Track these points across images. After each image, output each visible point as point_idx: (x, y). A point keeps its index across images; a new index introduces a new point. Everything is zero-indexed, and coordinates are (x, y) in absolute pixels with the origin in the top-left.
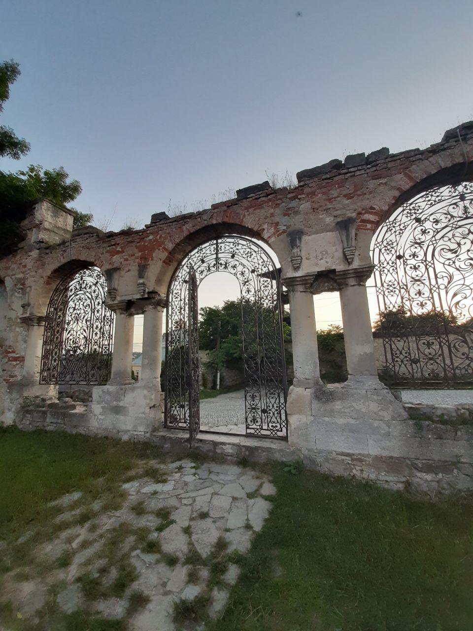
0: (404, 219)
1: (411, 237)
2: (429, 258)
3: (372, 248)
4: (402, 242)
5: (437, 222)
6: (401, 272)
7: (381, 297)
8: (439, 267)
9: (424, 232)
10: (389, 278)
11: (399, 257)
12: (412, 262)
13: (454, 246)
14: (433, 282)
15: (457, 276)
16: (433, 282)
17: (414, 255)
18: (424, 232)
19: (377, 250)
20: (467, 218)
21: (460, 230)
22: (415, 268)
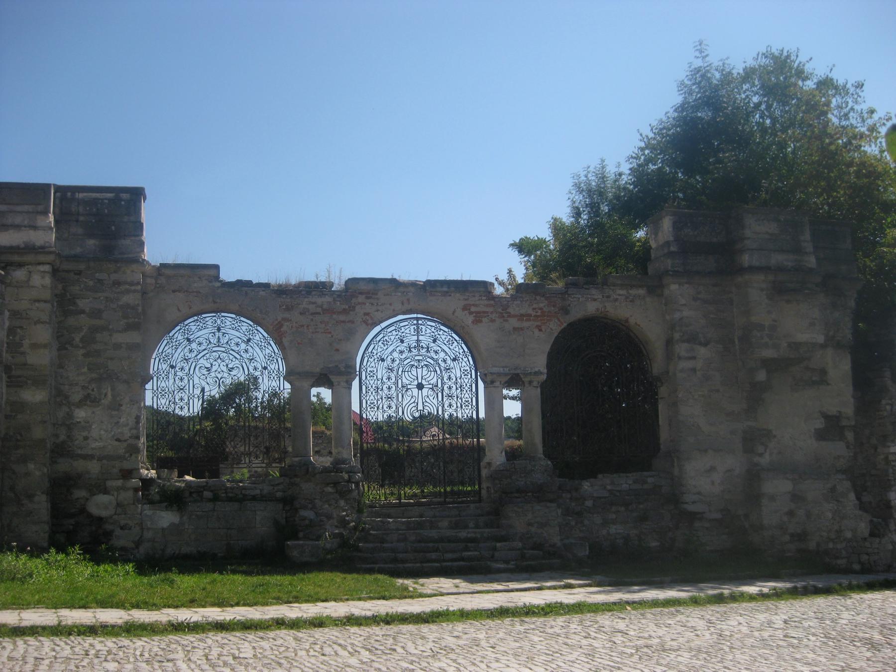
0: (180, 337)
1: (182, 354)
2: (191, 372)
3: (154, 357)
4: (176, 355)
5: (200, 344)
6: (171, 381)
7: (155, 398)
8: (196, 380)
9: (191, 351)
10: (163, 384)
11: (172, 367)
12: (180, 374)
13: (209, 366)
14: (191, 392)
15: (207, 389)
16: (191, 392)
17: (182, 369)
18: (191, 351)
19: (157, 359)
20: (219, 346)
21: (214, 354)
22: (181, 379)
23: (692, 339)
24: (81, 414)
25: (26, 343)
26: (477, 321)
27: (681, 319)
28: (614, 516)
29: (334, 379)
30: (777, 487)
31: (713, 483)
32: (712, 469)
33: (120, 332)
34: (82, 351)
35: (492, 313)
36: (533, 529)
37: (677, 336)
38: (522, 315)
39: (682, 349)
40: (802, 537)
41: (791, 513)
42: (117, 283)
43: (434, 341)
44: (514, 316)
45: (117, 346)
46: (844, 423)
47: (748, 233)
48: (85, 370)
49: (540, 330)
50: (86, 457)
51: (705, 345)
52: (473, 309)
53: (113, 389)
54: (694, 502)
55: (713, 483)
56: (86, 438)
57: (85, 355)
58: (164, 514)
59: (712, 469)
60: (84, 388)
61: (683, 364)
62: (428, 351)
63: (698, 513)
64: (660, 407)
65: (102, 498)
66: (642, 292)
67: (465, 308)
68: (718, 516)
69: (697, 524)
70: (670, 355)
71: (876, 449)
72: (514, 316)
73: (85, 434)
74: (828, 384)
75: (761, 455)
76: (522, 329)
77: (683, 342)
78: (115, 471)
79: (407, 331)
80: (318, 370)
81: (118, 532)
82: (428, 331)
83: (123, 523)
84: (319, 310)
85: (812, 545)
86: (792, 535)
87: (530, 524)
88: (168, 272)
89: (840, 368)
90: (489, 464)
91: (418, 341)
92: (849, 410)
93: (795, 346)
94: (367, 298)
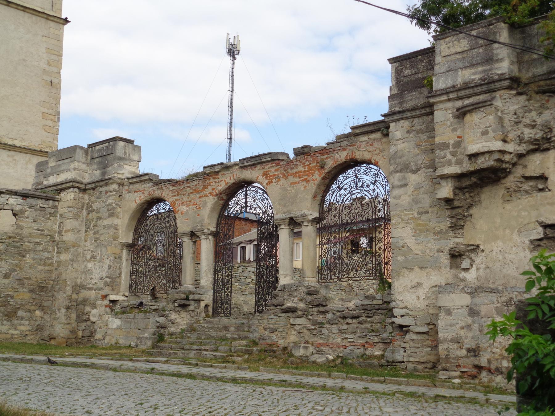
24: (90, 265)
25: (63, 231)
27: (396, 153)
28: (345, 327)
31: (418, 298)
32: (419, 285)
33: (105, 219)
34: (93, 232)
35: (278, 175)
36: (267, 333)
38: (296, 172)
41: (468, 327)
42: (107, 192)
43: (254, 201)
44: (292, 174)
45: (104, 227)
48: (93, 241)
49: (307, 181)
50: (91, 289)
53: (101, 251)
54: (402, 316)
55: (418, 298)
56: (91, 279)
57: (94, 234)
59: (419, 285)
60: (92, 251)
62: (251, 209)
63: (406, 326)
65: (94, 311)
68: (425, 329)
72: (292, 174)
73: (91, 276)
74: (550, 190)
75: (466, 270)
76: (295, 183)
77: (397, 172)
78: (100, 296)
79: (240, 197)
81: (98, 330)
82: (252, 194)
83: (100, 325)
84: (192, 191)
85: (483, 362)
86: (469, 350)
87: (265, 329)
88: (131, 181)
91: (246, 202)
93: (473, 156)
94: (214, 178)
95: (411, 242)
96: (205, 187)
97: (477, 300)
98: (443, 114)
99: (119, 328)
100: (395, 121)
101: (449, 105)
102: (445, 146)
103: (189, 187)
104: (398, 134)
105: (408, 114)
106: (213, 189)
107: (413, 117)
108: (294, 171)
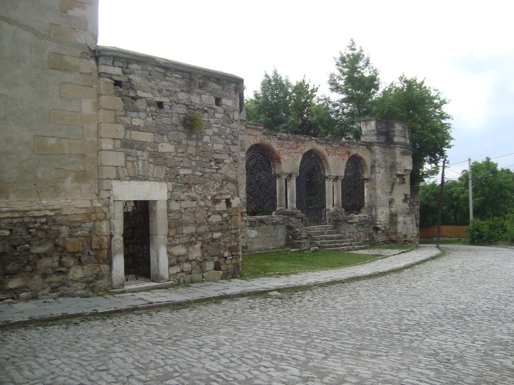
23: (379, 166)
26: (328, 155)
28: (360, 229)
29: (293, 175)
30: (400, 219)
37: (376, 165)
39: (377, 169)
40: (405, 236)
41: (403, 228)
46: (408, 197)
47: (396, 130)
51: (382, 168)
52: (329, 150)
58: (253, 231)
61: (378, 175)
64: (366, 190)
66: (365, 147)
67: (326, 150)
68: (383, 229)
69: (379, 232)
70: (373, 171)
71: (414, 206)
80: (289, 172)
89: (408, 179)
90: (328, 210)
92: (409, 193)
94: (302, 143)
95: (381, 195)
96: (298, 147)
97: (406, 219)
98: (398, 151)
99: (257, 237)
100: (377, 146)
101: (399, 149)
102: (398, 163)
103: (288, 144)
104: (378, 151)
105: (382, 145)
106: (302, 150)
107: (382, 146)
108: (338, 152)
